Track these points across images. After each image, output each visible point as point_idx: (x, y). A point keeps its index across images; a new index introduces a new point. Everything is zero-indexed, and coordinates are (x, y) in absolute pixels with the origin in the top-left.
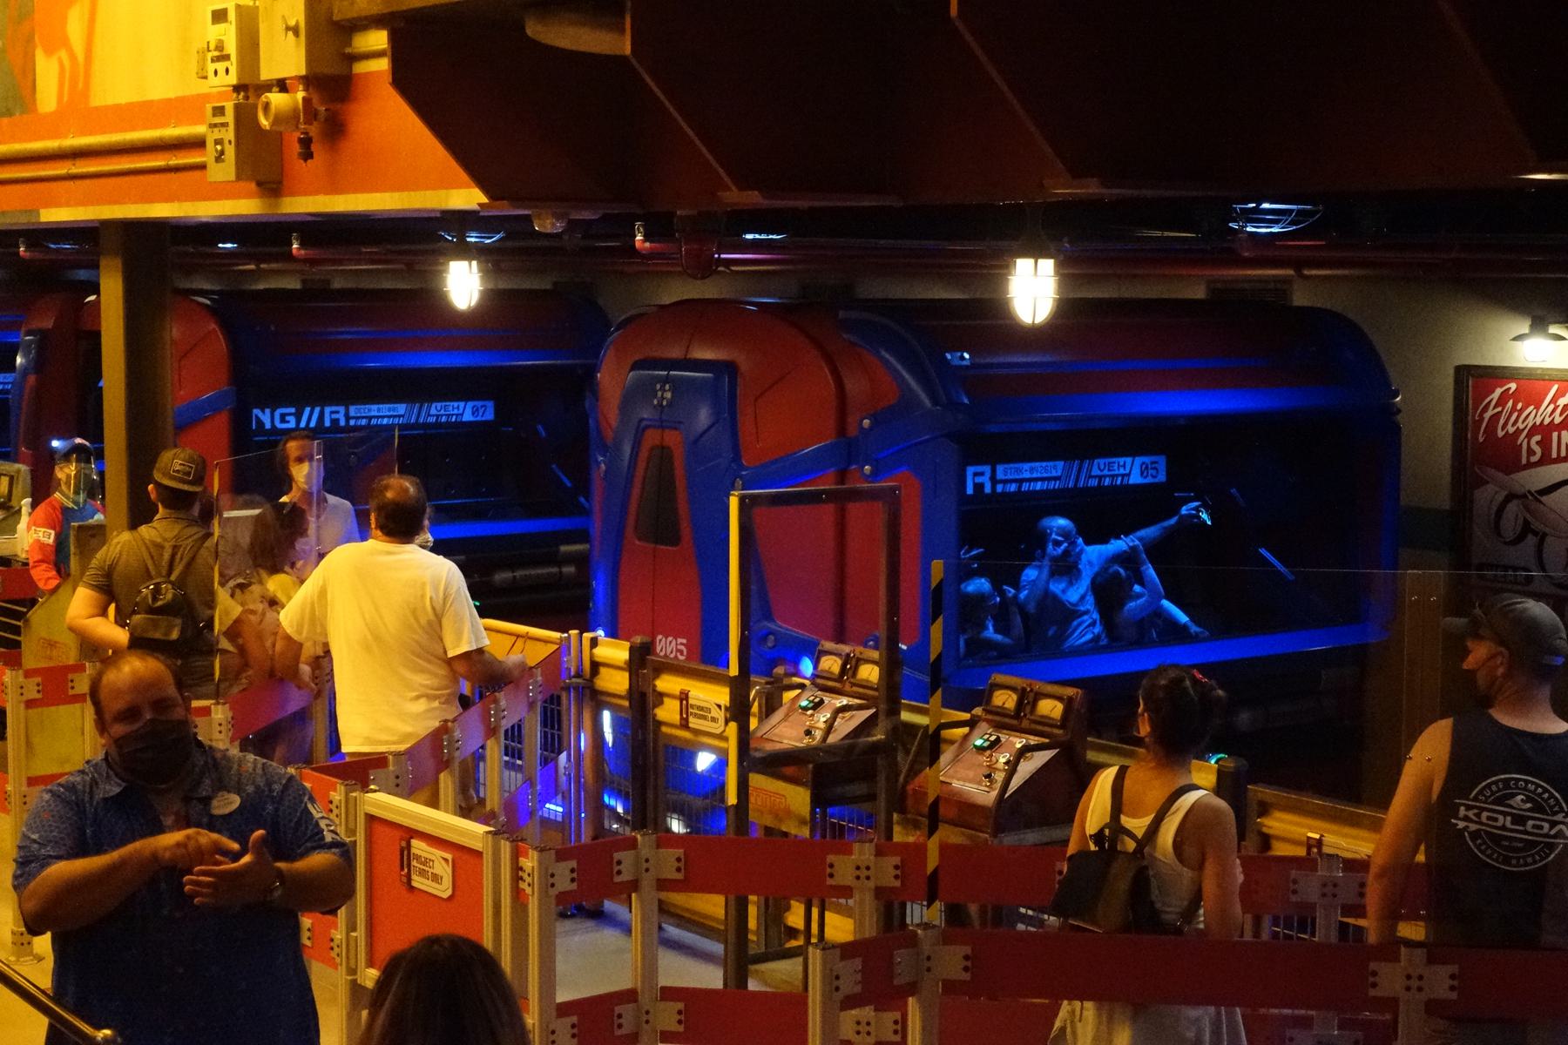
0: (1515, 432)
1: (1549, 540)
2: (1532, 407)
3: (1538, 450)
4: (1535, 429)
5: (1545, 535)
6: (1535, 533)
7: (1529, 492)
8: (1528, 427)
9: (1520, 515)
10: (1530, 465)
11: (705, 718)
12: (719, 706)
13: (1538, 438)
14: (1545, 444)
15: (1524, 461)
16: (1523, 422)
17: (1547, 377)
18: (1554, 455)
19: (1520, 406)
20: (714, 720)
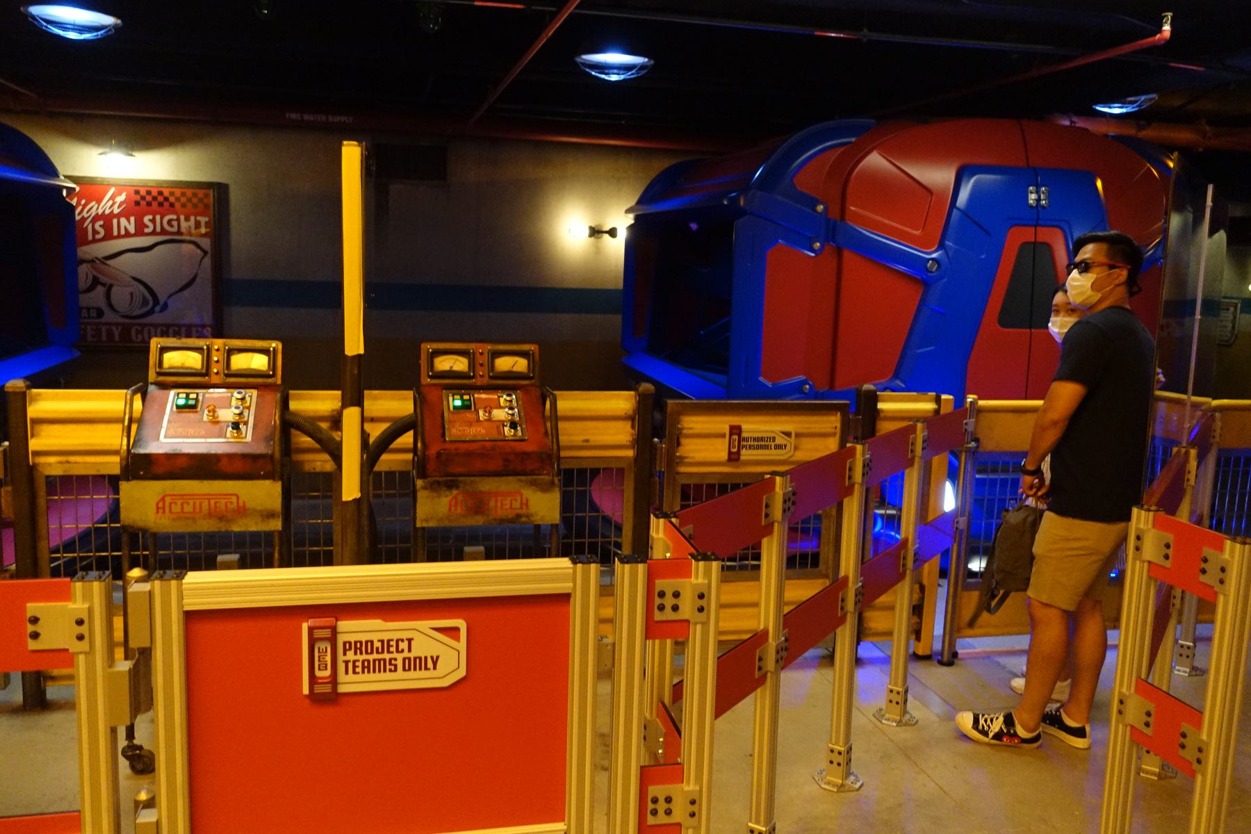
0: (81, 219)
1: (114, 289)
2: (94, 203)
3: (102, 232)
4: (97, 218)
5: (111, 286)
6: (104, 285)
7: (96, 258)
8: (92, 217)
9: (89, 273)
10: (95, 241)
11: (766, 447)
12: (788, 434)
13: (101, 223)
14: (108, 227)
15: (90, 237)
16: (88, 212)
17: (106, 183)
18: (115, 233)
19: (83, 202)
20: (778, 447)
